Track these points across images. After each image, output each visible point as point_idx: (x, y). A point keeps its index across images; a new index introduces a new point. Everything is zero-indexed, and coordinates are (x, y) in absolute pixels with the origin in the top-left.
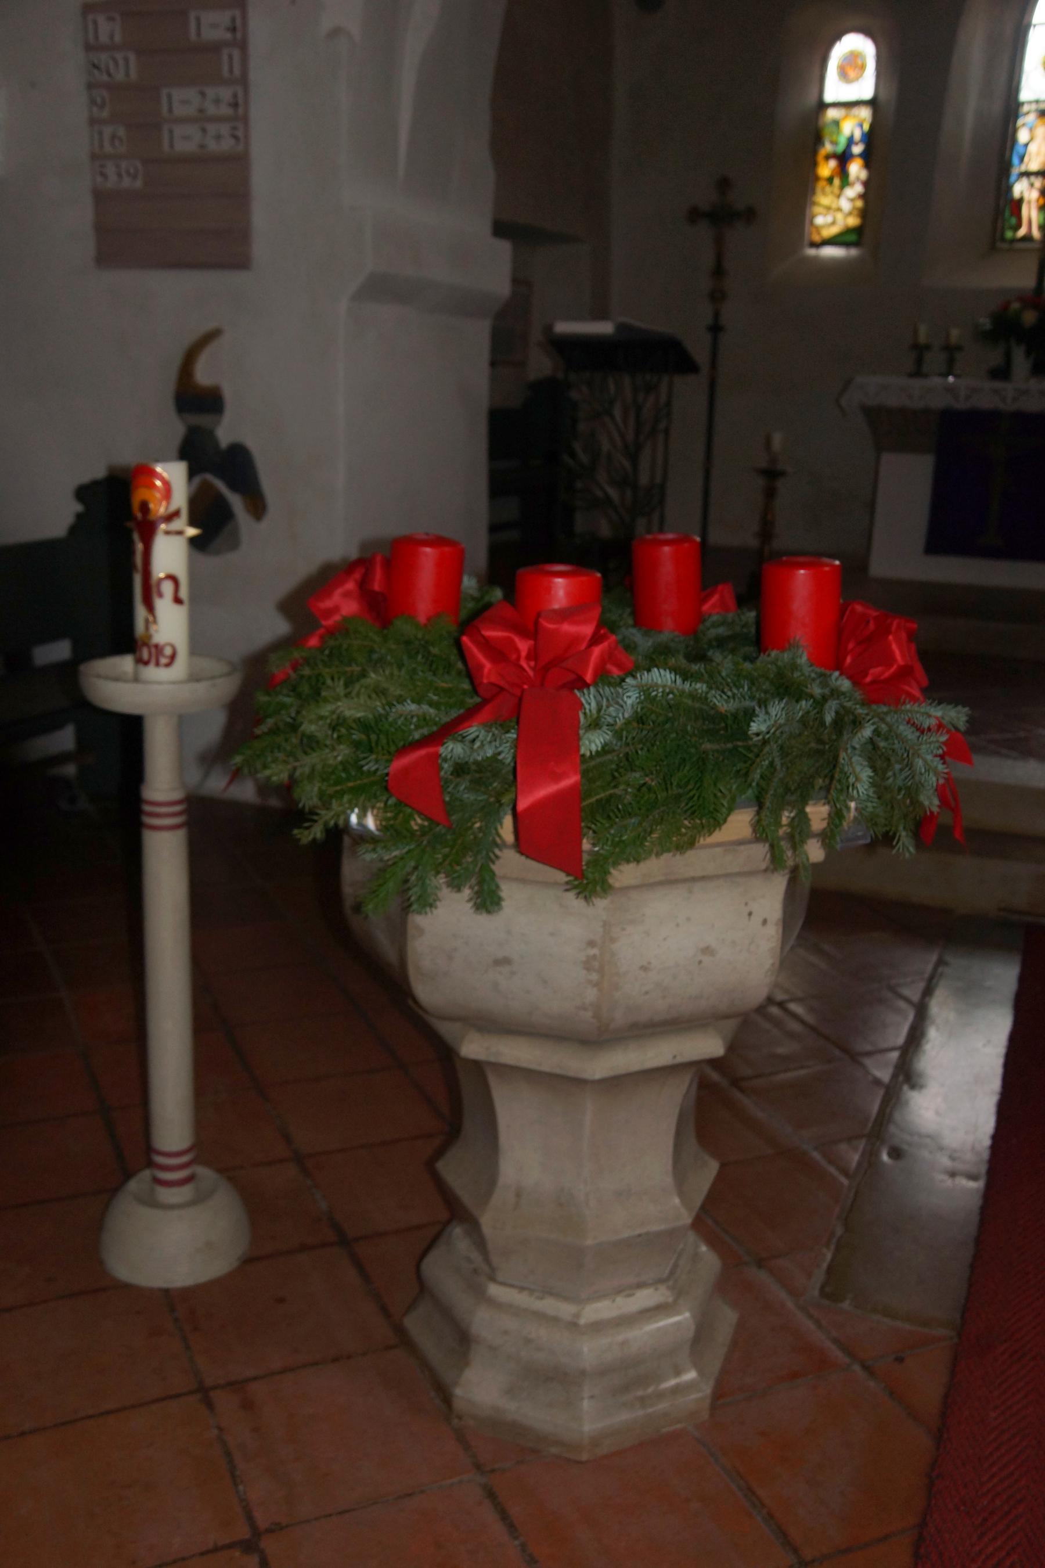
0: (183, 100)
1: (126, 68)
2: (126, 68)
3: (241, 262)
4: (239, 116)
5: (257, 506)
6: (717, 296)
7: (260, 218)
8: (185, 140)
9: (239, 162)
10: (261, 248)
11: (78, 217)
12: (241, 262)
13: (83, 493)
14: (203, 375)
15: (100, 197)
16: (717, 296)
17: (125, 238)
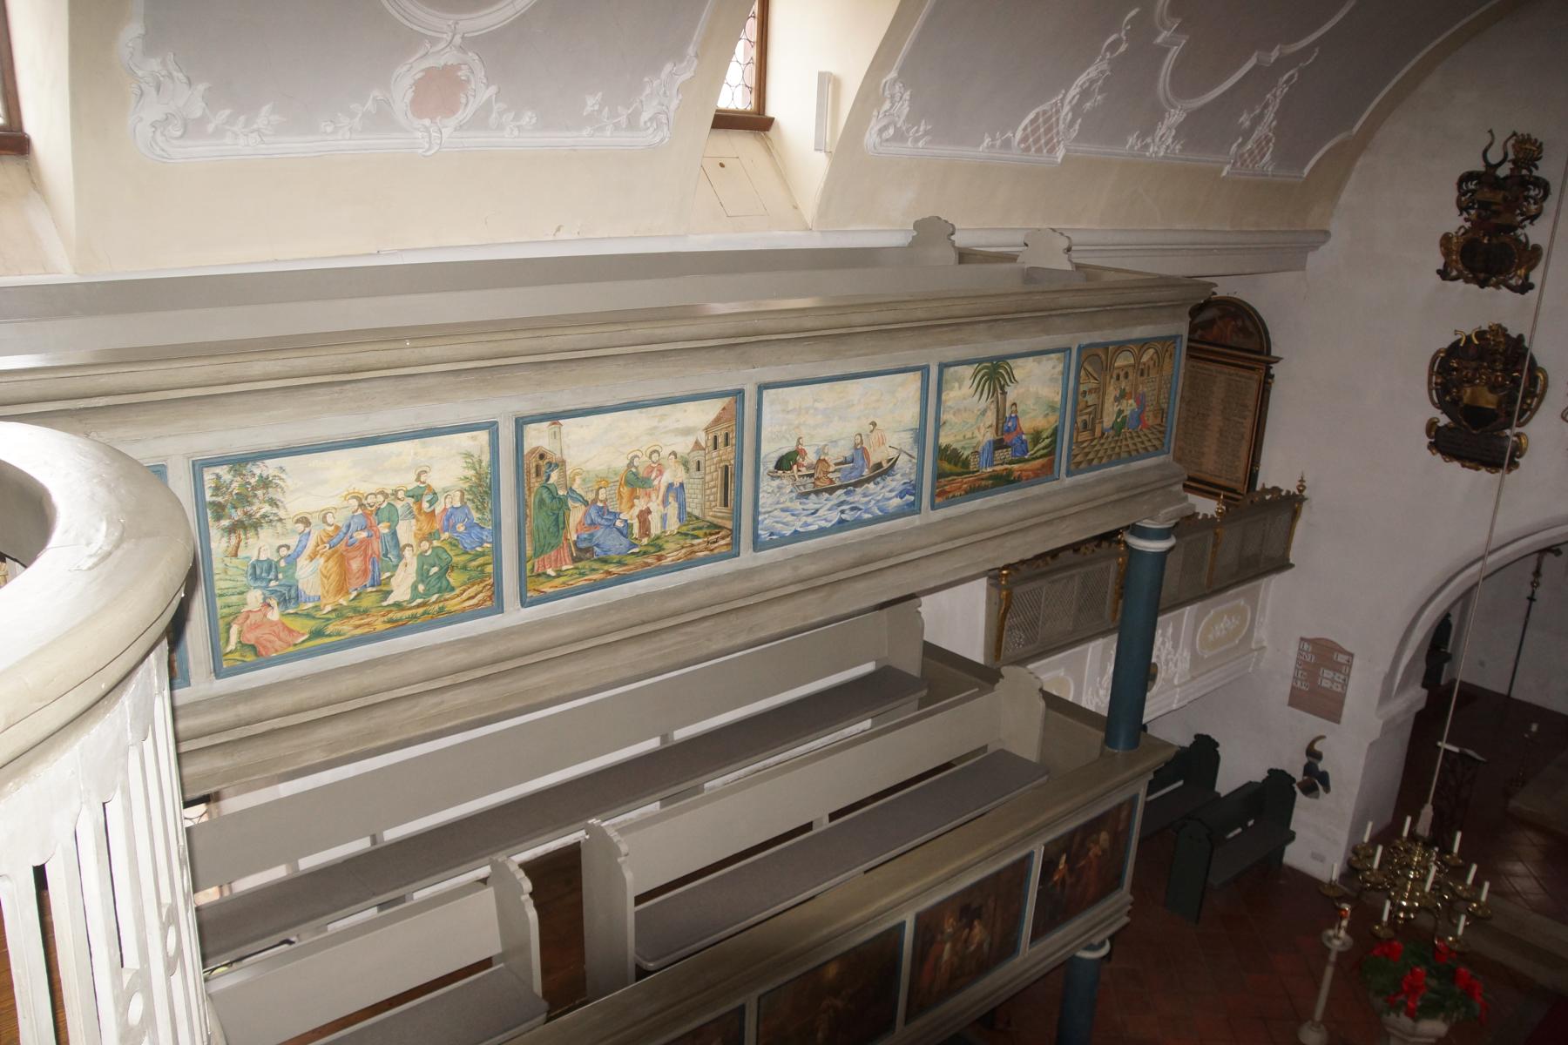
0: (1328, 674)
1: (1311, 659)
2: (1311, 659)
3: (1338, 721)
4: (1345, 685)
5: (1327, 789)
6: (1535, 584)
7: (1346, 711)
8: (1326, 684)
9: (1344, 696)
10: (1344, 719)
11: (1286, 689)
12: (1338, 721)
13: (1271, 771)
14: (1317, 747)
15: (1293, 688)
16: (1535, 584)
17: (1296, 700)
